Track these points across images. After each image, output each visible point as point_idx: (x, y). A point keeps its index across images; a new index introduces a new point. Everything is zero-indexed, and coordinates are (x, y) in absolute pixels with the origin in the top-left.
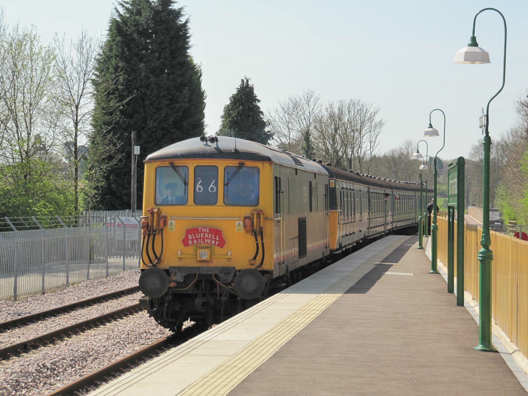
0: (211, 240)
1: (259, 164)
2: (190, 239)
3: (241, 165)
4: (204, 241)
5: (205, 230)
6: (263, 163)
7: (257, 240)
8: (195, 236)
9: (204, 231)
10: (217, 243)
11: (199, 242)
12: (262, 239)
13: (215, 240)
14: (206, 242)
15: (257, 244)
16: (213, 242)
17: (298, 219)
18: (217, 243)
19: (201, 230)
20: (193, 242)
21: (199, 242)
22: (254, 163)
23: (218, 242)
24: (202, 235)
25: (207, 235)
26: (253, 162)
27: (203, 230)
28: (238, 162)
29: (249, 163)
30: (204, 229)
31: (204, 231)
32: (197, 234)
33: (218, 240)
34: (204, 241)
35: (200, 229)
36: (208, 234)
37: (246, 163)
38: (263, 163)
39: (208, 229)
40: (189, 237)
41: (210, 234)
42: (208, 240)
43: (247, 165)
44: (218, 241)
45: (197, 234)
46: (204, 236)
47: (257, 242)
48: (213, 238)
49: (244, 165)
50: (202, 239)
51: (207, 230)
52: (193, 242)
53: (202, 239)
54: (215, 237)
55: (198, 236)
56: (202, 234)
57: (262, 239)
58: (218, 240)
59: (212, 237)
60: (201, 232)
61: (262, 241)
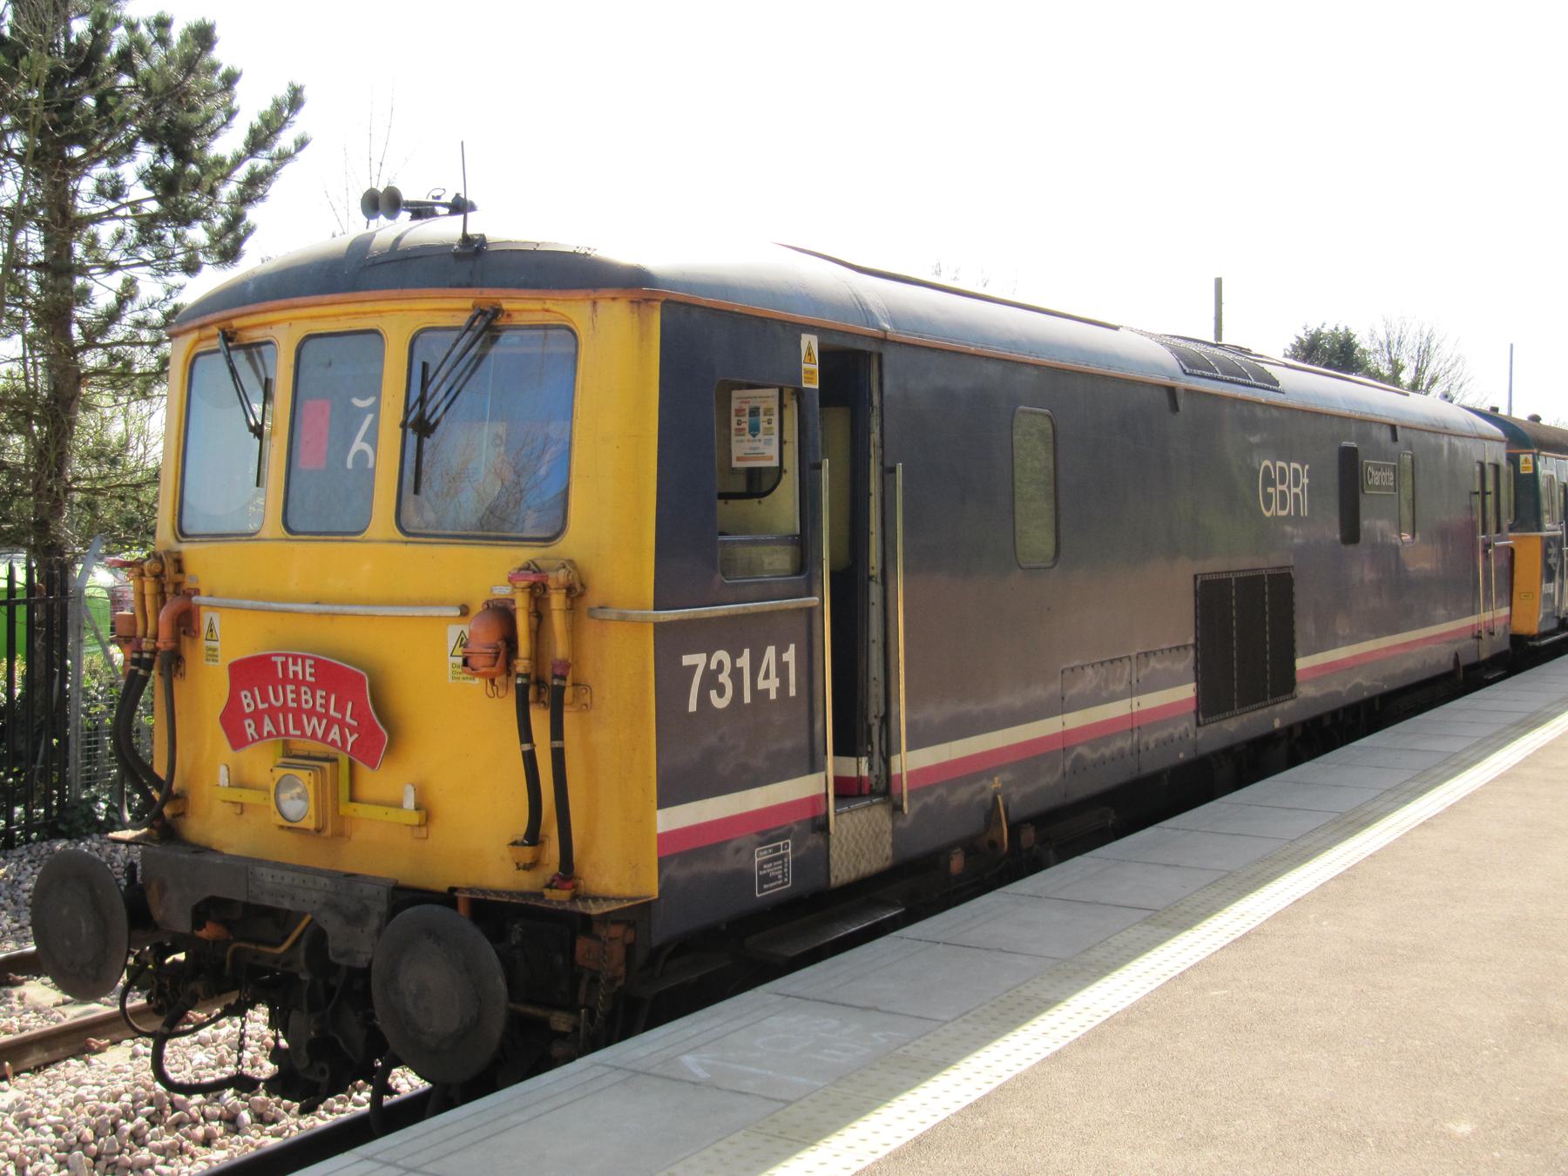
0: (324, 721)
1: (573, 310)
2: (248, 710)
3: (488, 325)
4: (298, 725)
5: (299, 669)
6: (595, 303)
7: (526, 734)
8: (265, 699)
9: (295, 673)
10: (351, 740)
11: (283, 731)
12: (557, 732)
13: (342, 724)
14: (309, 732)
15: (530, 760)
16: (335, 734)
17: (1195, 577)
18: (351, 740)
19: (285, 665)
20: (259, 729)
21: (283, 731)
22: (549, 305)
23: (356, 736)
24: (290, 696)
25: (308, 697)
26: (544, 300)
27: (291, 668)
28: (468, 304)
29: (523, 307)
30: (295, 663)
31: (295, 673)
32: (270, 688)
33: (355, 723)
34: (298, 725)
35: (279, 660)
36: (313, 688)
37: (506, 305)
38: (595, 303)
39: (309, 662)
40: (245, 702)
41: (320, 693)
42: (315, 721)
43: (518, 319)
44: (352, 730)
45: (270, 688)
46: (297, 700)
47: (557, 744)
48: (332, 712)
49: (502, 321)
50: (290, 716)
51: (308, 670)
52: (259, 729)
53: (290, 716)
54: (340, 707)
55: (277, 699)
56: (290, 688)
57: (557, 732)
58: (355, 723)
59: (326, 706)
60: (286, 680)
61: (527, 747)
